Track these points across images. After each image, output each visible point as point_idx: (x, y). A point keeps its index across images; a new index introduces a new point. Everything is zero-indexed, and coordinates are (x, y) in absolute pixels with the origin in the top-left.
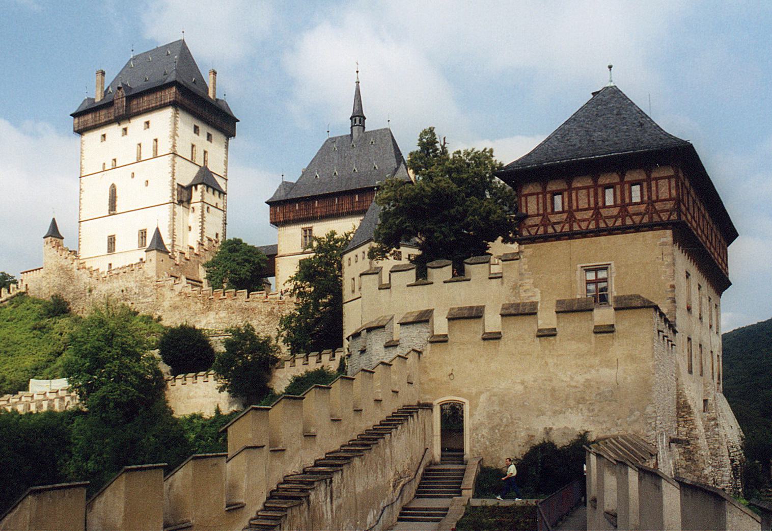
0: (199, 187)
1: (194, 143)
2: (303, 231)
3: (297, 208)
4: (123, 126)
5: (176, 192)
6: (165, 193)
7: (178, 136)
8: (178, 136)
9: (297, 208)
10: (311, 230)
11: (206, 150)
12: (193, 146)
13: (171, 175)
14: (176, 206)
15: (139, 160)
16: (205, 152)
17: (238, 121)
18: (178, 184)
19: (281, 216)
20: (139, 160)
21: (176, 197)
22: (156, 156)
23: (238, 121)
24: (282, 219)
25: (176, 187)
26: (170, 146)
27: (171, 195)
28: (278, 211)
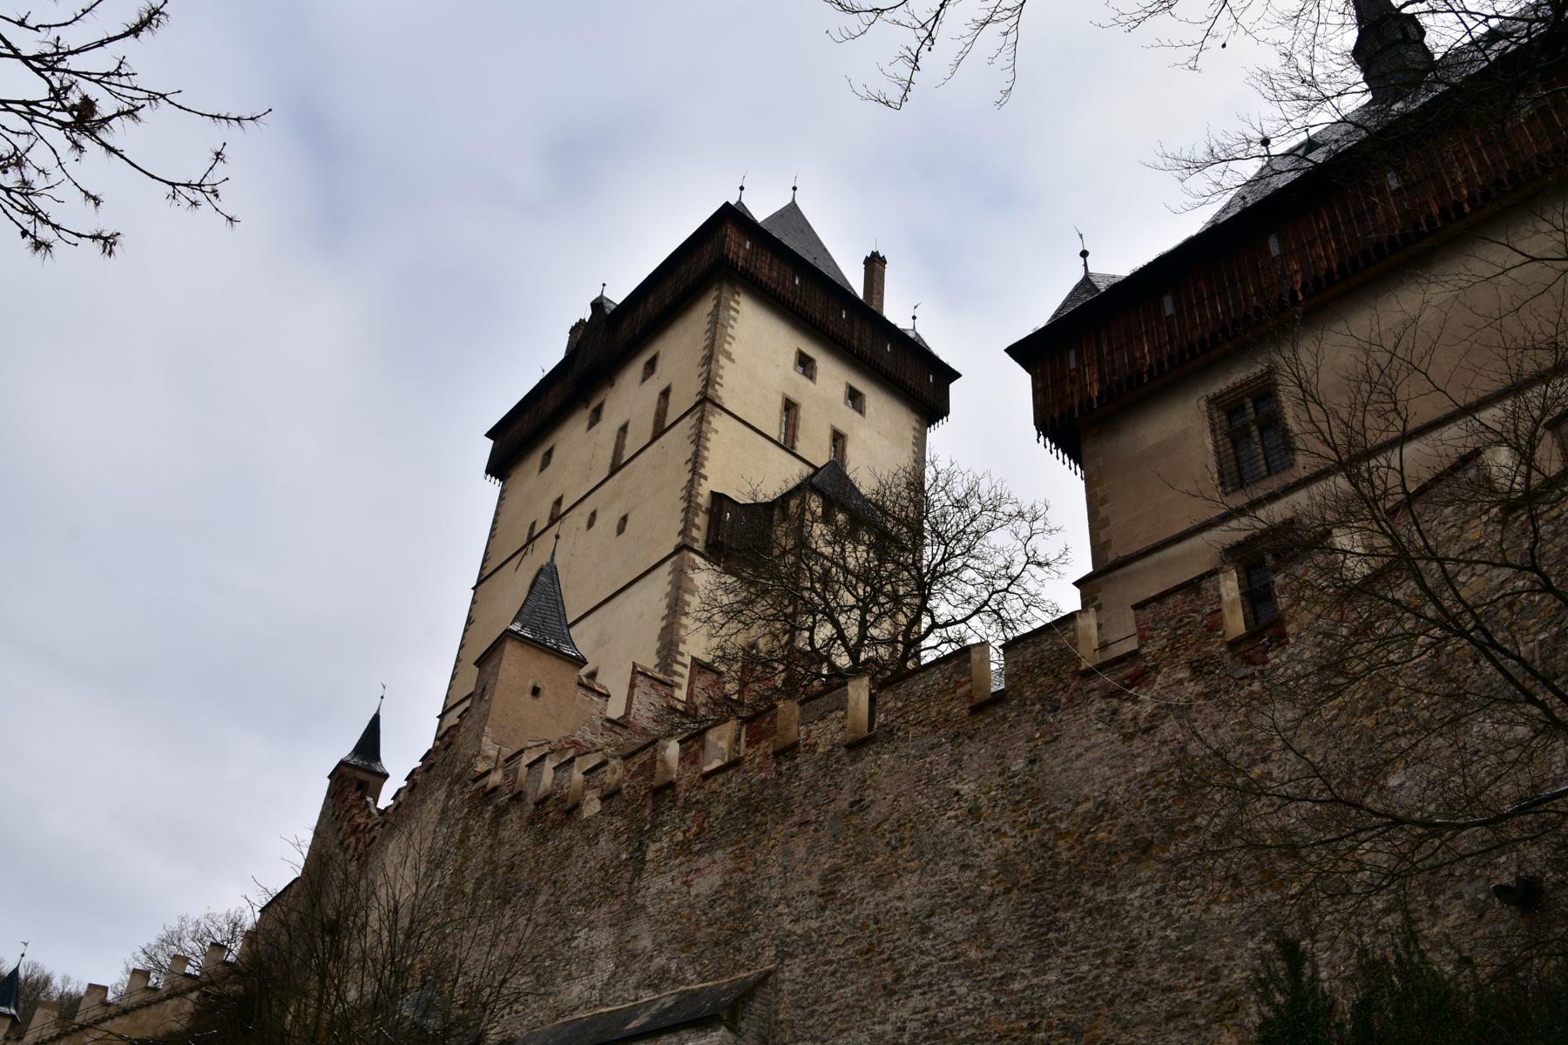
0: (793, 503)
1: (793, 396)
2: (1220, 417)
3: (1169, 309)
4: (594, 405)
5: (701, 520)
6: (660, 526)
7: (733, 361)
8: (733, 361)
9: (1169, 309)
10: (1264, 392)
11: (842, 428)
12: (790, 407)
13: (690, 466)
14: (699, 560)
15: (616, 468)
16: (838, 438)
17: (956, 375)
18: (717, 498)
19: (1091, 377)
20: (616, 468)
21: (699, 536)
22: (659, 430)
23: (955, 375)
24: (1094, 391)
25: (703, 500)
26: (697, 385)
27: (681, 526)
28: (1073, 365)
